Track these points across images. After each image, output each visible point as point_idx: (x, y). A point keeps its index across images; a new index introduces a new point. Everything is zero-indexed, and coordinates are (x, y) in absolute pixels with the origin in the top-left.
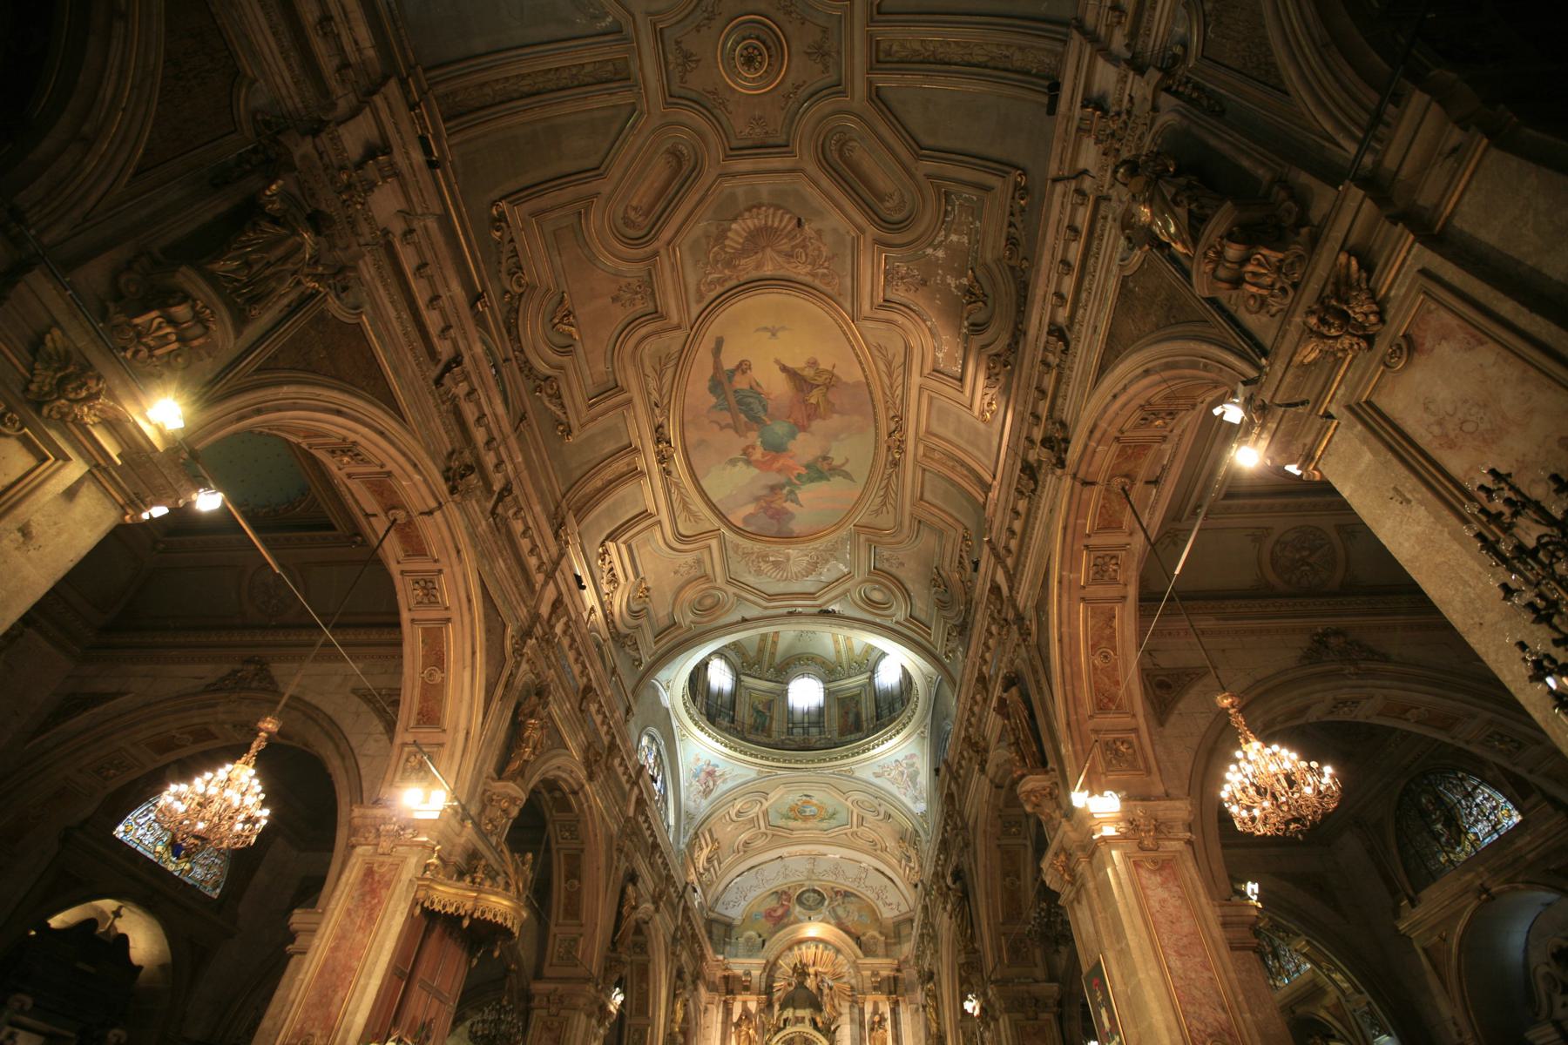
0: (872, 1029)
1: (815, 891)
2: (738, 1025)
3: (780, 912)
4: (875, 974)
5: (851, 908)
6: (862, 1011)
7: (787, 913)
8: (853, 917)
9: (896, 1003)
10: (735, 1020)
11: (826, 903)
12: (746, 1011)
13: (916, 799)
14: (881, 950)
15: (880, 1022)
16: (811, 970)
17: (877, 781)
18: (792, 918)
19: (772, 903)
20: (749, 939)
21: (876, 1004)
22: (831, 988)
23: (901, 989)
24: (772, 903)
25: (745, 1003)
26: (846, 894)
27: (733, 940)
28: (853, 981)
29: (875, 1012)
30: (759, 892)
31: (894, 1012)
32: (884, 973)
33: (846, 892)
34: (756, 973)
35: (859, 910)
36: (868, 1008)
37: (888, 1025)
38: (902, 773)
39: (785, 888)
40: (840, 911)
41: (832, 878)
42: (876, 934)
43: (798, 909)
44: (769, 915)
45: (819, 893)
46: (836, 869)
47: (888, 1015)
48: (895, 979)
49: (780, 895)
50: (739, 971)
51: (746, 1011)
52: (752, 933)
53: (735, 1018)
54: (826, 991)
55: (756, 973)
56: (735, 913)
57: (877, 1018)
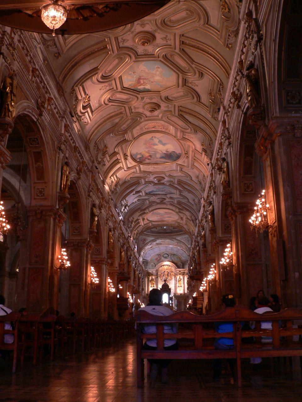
0: (179, 281)
1: (167, 254)
2: (151, 281)
3: (159, 259)
4: (180, 272)
5: (175, 258)
6: (177, 278)
7: (160, 259)
8: (175, 259)
9: (184, 277)
10: (150, 280)
11: (169, 256)
12: (152, 278)
13: (189, 245)
14: (181, 267)
15: (180, 280)
16: (166, 271)
17: (181, 240)
18: (162, 260)
19: (157, 257)
20: (152, 265)
21: (180, 277)
22: (170, 274)
23: (185, 274)
24: (157, 257)
25: (152, 277)
26: (174, 255)
27: (148, 265)
28: (175, 273)
29: (180, 278)
30: (154, 254)
31: (184, 278)
32: (181, 271)
33: (174, 254)
34: (154, 272)
35: (177, 258)
36: (178, 277)
37: (182, 280)
38: (186, 240)
39: (160, 253)
40: (173, 258)
41: (171, 251)
42: (180, 263)
43: (163, 258)
44: (156, 259)
45: (168, 255)
46: (172, 249)
47: (182, 278)
48: (184, 272)
49: (159, 255)
50: (150, 271)
51: (152, 278)
52: (152, 264)
53: (150, 280)
54: (169, 275)
55: (154, 272)
56: (149, 259)
57: (180, 279)
